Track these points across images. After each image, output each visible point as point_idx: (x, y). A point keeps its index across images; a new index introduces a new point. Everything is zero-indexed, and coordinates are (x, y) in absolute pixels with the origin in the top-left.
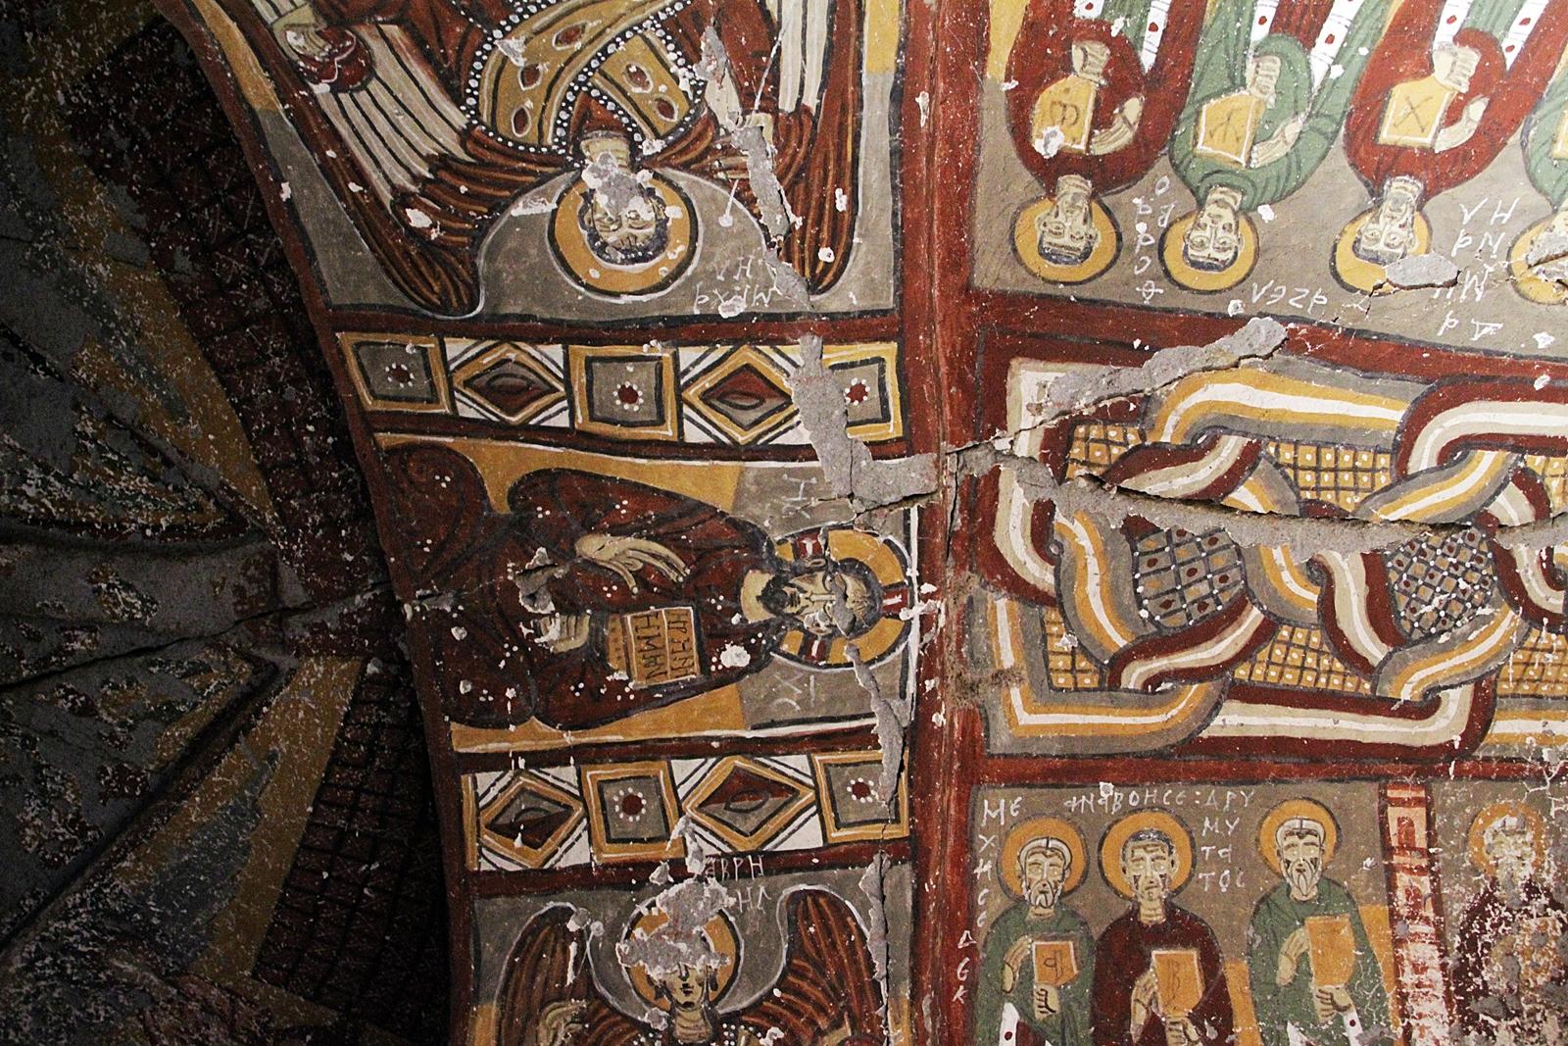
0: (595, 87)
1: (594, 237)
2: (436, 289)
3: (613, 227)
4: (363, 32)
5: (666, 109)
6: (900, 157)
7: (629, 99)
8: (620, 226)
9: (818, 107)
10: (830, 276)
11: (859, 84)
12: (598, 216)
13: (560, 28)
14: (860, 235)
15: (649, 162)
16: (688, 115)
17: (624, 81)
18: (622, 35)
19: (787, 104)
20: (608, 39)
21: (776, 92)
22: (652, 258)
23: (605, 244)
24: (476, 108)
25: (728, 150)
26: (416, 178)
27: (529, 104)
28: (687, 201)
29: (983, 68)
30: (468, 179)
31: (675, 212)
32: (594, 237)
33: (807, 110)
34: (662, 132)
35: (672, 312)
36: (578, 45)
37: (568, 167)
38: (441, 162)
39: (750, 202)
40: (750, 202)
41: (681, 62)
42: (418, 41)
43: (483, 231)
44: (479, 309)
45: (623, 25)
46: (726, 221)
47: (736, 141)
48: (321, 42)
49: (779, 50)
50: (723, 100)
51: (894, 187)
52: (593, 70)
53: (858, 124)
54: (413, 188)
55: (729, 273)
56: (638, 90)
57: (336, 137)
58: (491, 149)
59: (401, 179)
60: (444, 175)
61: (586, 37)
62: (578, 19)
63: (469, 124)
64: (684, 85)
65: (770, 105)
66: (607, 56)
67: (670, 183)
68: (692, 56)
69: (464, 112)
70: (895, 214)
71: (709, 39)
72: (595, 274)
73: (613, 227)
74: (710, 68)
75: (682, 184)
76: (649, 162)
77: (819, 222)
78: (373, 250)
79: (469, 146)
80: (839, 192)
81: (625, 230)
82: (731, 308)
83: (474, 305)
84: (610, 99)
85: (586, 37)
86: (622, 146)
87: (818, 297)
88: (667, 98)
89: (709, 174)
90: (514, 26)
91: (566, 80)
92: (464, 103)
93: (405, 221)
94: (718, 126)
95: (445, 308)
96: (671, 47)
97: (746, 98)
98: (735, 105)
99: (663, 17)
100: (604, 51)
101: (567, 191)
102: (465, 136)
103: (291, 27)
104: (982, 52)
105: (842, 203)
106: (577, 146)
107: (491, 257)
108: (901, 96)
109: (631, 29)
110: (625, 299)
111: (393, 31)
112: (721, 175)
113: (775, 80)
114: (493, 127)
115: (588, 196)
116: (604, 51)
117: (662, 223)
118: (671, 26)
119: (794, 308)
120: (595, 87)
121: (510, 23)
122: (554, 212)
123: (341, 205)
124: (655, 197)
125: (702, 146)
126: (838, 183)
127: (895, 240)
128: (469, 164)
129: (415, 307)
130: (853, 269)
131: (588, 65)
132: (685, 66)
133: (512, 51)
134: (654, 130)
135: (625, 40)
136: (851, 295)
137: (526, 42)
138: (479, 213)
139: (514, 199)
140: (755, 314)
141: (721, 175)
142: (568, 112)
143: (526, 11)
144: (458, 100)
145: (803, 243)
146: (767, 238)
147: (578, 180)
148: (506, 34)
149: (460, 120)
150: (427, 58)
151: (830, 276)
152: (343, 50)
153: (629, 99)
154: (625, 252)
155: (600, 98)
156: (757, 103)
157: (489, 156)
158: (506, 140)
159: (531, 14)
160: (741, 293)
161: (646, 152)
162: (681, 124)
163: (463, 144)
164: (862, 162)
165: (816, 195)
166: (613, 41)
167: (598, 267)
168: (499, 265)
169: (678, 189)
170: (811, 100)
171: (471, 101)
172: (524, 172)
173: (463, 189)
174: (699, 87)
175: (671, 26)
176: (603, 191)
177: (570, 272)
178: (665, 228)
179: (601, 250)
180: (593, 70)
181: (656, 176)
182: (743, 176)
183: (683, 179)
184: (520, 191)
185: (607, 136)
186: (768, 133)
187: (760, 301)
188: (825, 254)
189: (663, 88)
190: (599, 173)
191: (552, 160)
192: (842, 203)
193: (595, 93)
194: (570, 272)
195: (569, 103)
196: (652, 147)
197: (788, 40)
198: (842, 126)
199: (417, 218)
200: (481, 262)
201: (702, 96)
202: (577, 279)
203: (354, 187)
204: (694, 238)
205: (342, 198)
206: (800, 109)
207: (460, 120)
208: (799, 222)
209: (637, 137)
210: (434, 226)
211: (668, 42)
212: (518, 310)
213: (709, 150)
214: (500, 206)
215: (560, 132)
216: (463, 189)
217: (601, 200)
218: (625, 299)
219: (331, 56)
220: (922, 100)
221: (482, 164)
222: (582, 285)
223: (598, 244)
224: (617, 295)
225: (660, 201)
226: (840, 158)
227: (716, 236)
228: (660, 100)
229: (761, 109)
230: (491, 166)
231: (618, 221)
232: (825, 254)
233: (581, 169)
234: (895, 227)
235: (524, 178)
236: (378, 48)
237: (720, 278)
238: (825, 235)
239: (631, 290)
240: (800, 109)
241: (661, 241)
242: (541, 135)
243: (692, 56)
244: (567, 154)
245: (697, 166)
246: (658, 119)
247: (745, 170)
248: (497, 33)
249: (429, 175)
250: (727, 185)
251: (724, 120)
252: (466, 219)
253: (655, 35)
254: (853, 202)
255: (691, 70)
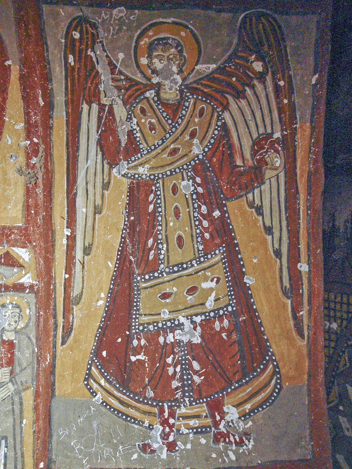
0: (170, 124)
1: (180, 52)
2: (261, 25)
3: (172, 56)
4: (250, 163)
5: (143, 111)
6: (47, 78)
7: (157, 117)
8: (168, 57)
9: (82, 104)
10: (74, 25)
11: (67, 113)
12: (177, 62)
13: (177, 156)
14: (62, 43)
15: (152, 86)
16: (134, 107)
17: (157, 127)
18: (156, 148)
19: (95, 107)
20: (161, 147)
21: (99, 112)
22: (155, 40)
23: (176, 48)
24: (218, 120)
25: (119, 88)
26: (253, 87)
27: (196, 120)
28: (138, 66)
29: (21, 70)
30: (230, 85)
31: (144, 61)
32: (180, 52)
33: (87, 103)
34: (145, 101)
35: (148, 12)
36: (172, 146)
37: (187, 87)
38: (239, 95)
39: (110, 63)
40: (110, 63)
41: (135, 132)
42: (231, 156)
43: (230, 58)
44: (243, 15)
45: (154, 153)
46: (121, 56)
47: (116, 92)
48: (268, 160)
49: (98, 132)
50: (120, 112)
51: (49, 64)
52: (169, 133)
53: (66, 95)
54: (256, 82)
55: (120, 29)
56: (153, 121)
57: (280, 111)
58: (216, 100)
59: (259, 87)
60: (240, 88)
61: (168, 150)
62: (170, 159)
63: (223, 112)
64: (135, 121)
65: (102, 107)
66: (162, 139)
67: (145, 76)
68: (130, 133)
69: (223, 119)
70: (48, 51)
71: (124, 139)
72: (183, 34)
73: (172, 56)
74: (124, 126)
75: (139, 75)
76: (152, 86)
77: (80, 51)
78: (285, 47)
79: (225, 103)
80: (73, 64)
81: (166, 55)
82: (120, 11)
83: (245, 17)
84: (164, 118)
85: (168, 150)
86: (163, 95)
87: (79, 14)
88: (142, 116)
89: (127, 78)
90: (194, 160)
91: (180, 128)
92: (222, 123)
93: (265, 67)
94: (123, 100)
95: (260, 15)
96: (138, 139)
97: (111, 111)
98: (115, 106)
99: (139, 155)
100: (163, 142)
101: (189, 74)
102: (226, 107)
103: (276, 169)
104: (22, 78)
105: (71, 58)
106: (181, 97)
107: (230, 44)
108: (50, 106)
109: (152, 150)
110: (170, 20)
111: (239, 162)
112: (122, 77)
113: (100, 118)
114: (214, 109)
115: (180, 72)
116: (163, 142)
117: (150, 57)
118: (137, 150)
119: (90, 9)
120: (170, 124)
121: (195, 161)
122: (196, 65)
123: (291, 73)
124: (151, 69)
125: (130, 92)
126: (73, 68)
127: (46, 38)
128: (228, 93)
129: (276, 16)
130: (64, 26)
131: (170, 135)
132: (134, 129)
133: (198, 147)
134: (148, 102)
135: (154, 145)
136: (63, 14)
137: (191, 151)
138: (230, 67)
139: (212, 72)
140: (109, 8)
141: (122, 77)
142: (182, 114)
143: (188, 166)
144: (225, 124)
145: (87, 42)
146: (103, 46)
147: (184, 80)
148: (197, 156)
149: (226, 115)
150: (231, 146)
151: (74, 25)
152: (262, 154)
153: (157, 117)
154: (166, 44)
155: (168, 119)
156: (107, 109)
157: (218, 96)
158: (210, 103)
159: (186, 164)
160: (115, 20)
161: (153, 91)
162: (138, 103)
163: (228, 103)
164: (63, 78)
165: (82, 64)
166: (159, 146)
167: (182, 37)
168: (227, 39)
169: (142, 72)
170: (85, 107)
171: (219, 123)
172: (206, 86)
173: (234, 79)
174: (129, 119)
175: (137, 150)
176: (174, 73)
177: (194, 35)
178: (148, 53)
179: (178, 45)
180: (169, 133)
181: (150, 80)
182: (113, 76)
183: (138, 77)
184: (210, 77)
185: (168, 100)
186: (102, 95)
187: (106, 14)
188: (77, 35)
189: (143, 121)
190: (174, 81)
191: (194, 91)
192: (71, 58)
193: (170, 122)
194: (194, 35)
195: (181, 118)
196: (150, 94)
197: (94, 137)
198: (72, 94)
199: (258, 66)
200: (235, 41)
201: (129, 114)
202: (192, 31)
203: (282, 83)
204: (136, 47)
205: (290, 77)
206: (90, 104)
207: (226, 115)
208: (89, 52)
209: (156, 99)
210: (252, 62)
211: (139, 141)
212: (223, 14)
213: (127, 90)
214: (221, 70)
215: (187, 104)
216: (234, 79)
217: (175, 69)
218: (170, 20)
219: (266, 152)
220: (42, 103)
221: (222, 93)
222: (190, 29)
223: (179, 48)
224: (174, 23)
225: (149, 67)
226: (73, 80)
227: (125, 49)
228: (145, 115)
229: (105, 105)
230: (217, 91)
231: (169, 59)
232: (77, 35)
233: (181, 85)
234: (46, 44)
235: (207, 83)
236: (248, 155)
237: (125, 28)
238: (78, 44)
239: (166, 25)
240: (90, 104)
241: (151, 48)
242: (195, 104)
243: (130, 133)
244: (186, 93)
245: (133, 83)
246: (146, 107)
247: (112, 79)
248: (201, 157)
249: (247, 88)
250: (121, 73)
251: (120, 102)
252: (236, 65)
253: (143, 146)
254: (66, 59)
255: (132, 127)
